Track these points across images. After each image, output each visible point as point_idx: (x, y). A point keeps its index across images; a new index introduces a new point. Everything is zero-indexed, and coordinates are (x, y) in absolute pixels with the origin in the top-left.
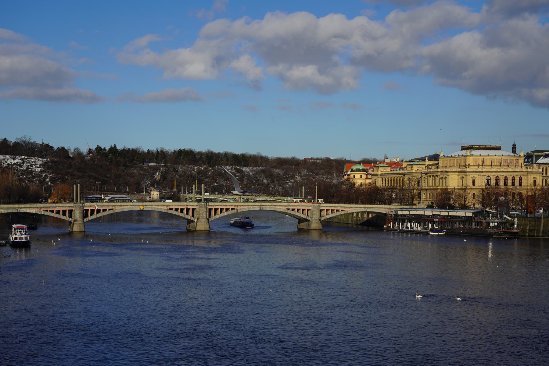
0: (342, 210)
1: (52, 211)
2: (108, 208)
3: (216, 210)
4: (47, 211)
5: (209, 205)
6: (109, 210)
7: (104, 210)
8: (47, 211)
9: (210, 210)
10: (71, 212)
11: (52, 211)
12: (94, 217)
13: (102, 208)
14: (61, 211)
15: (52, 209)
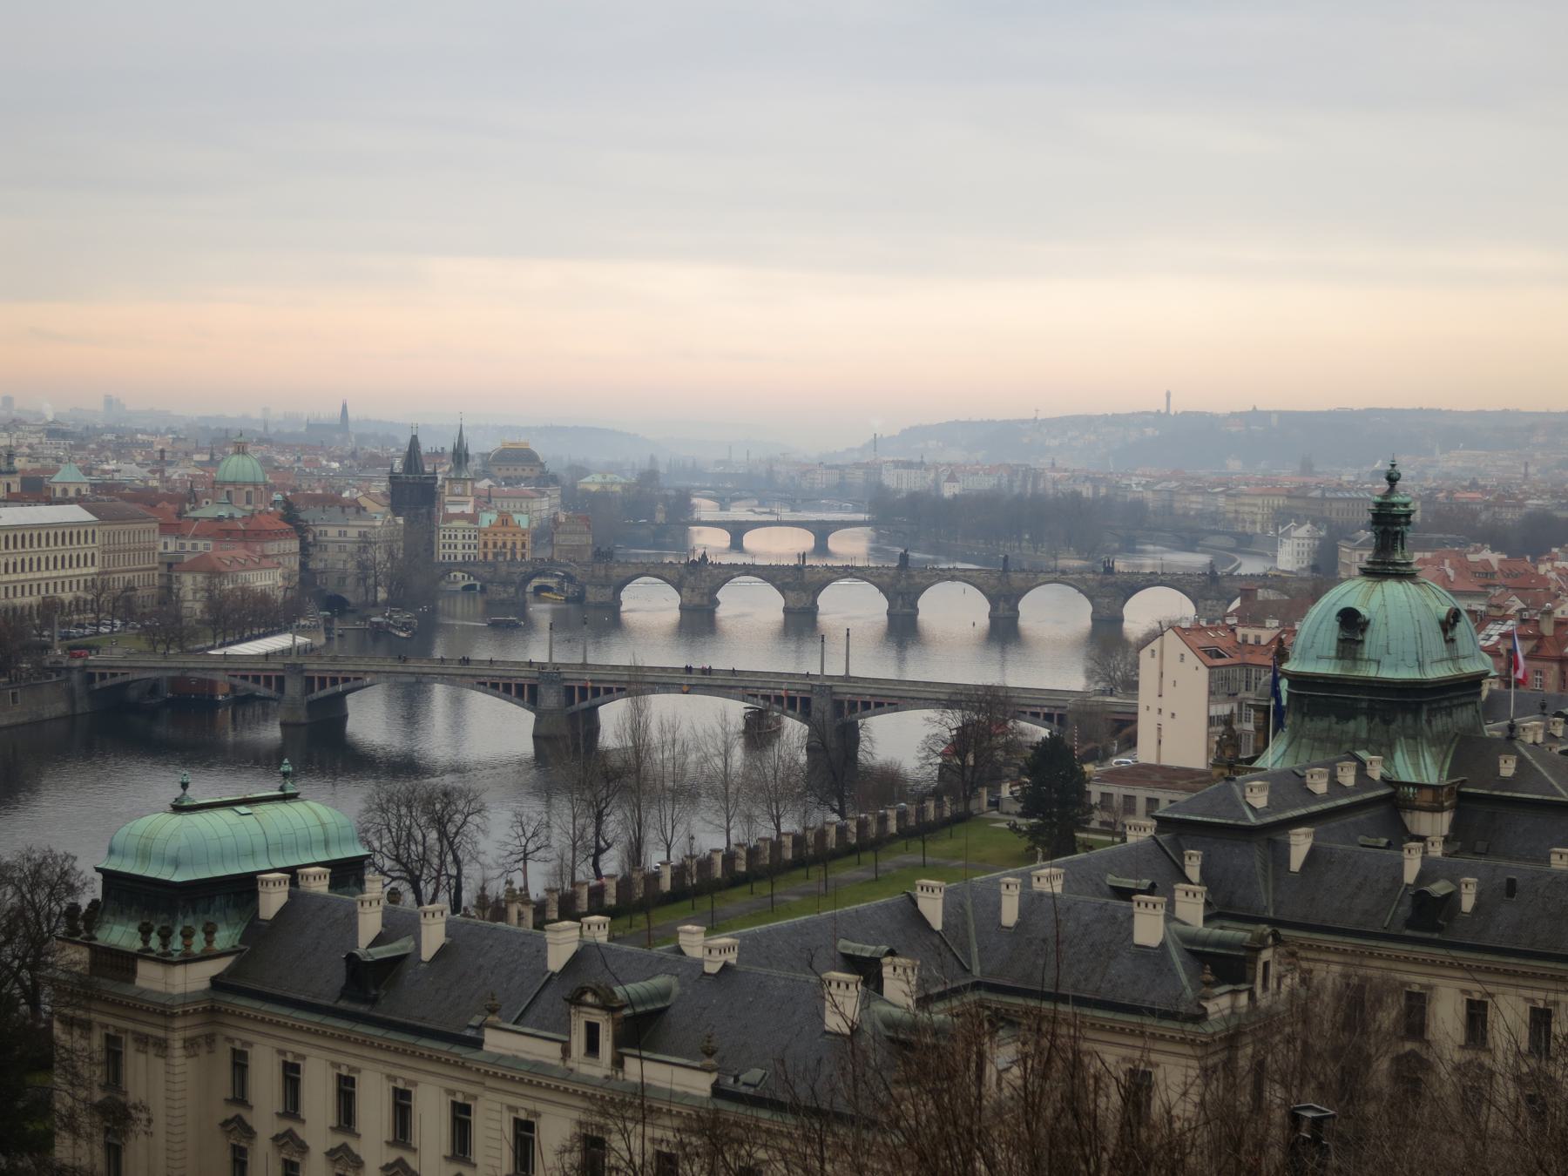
0: (889, 704)
1: (245, 678)
2: (352, 676)
3: (583, 690)
4: (235, 676)
5: (565, 680)
6: (356, 679)
7: (346, 680)
8: (235, 676)
9: (570, 690)
10: (281, 680)
11: (245, 678)
12: (322, 694)
13: (340, 676)
14: (262, 678)
15: (244, 673)
